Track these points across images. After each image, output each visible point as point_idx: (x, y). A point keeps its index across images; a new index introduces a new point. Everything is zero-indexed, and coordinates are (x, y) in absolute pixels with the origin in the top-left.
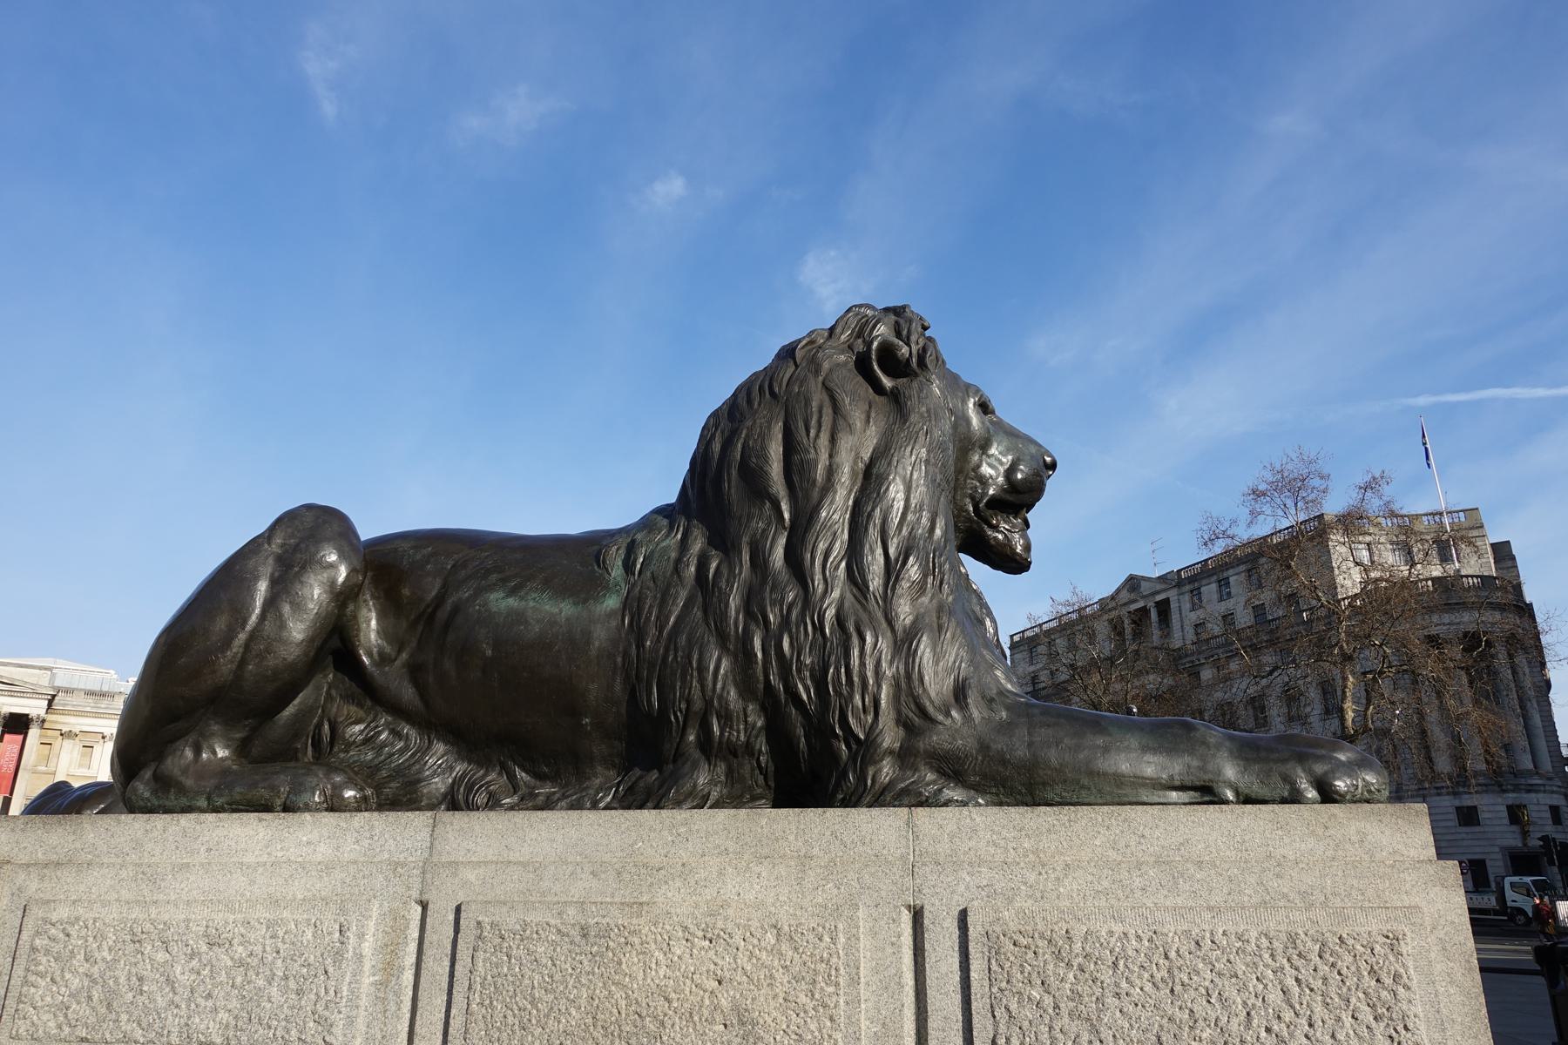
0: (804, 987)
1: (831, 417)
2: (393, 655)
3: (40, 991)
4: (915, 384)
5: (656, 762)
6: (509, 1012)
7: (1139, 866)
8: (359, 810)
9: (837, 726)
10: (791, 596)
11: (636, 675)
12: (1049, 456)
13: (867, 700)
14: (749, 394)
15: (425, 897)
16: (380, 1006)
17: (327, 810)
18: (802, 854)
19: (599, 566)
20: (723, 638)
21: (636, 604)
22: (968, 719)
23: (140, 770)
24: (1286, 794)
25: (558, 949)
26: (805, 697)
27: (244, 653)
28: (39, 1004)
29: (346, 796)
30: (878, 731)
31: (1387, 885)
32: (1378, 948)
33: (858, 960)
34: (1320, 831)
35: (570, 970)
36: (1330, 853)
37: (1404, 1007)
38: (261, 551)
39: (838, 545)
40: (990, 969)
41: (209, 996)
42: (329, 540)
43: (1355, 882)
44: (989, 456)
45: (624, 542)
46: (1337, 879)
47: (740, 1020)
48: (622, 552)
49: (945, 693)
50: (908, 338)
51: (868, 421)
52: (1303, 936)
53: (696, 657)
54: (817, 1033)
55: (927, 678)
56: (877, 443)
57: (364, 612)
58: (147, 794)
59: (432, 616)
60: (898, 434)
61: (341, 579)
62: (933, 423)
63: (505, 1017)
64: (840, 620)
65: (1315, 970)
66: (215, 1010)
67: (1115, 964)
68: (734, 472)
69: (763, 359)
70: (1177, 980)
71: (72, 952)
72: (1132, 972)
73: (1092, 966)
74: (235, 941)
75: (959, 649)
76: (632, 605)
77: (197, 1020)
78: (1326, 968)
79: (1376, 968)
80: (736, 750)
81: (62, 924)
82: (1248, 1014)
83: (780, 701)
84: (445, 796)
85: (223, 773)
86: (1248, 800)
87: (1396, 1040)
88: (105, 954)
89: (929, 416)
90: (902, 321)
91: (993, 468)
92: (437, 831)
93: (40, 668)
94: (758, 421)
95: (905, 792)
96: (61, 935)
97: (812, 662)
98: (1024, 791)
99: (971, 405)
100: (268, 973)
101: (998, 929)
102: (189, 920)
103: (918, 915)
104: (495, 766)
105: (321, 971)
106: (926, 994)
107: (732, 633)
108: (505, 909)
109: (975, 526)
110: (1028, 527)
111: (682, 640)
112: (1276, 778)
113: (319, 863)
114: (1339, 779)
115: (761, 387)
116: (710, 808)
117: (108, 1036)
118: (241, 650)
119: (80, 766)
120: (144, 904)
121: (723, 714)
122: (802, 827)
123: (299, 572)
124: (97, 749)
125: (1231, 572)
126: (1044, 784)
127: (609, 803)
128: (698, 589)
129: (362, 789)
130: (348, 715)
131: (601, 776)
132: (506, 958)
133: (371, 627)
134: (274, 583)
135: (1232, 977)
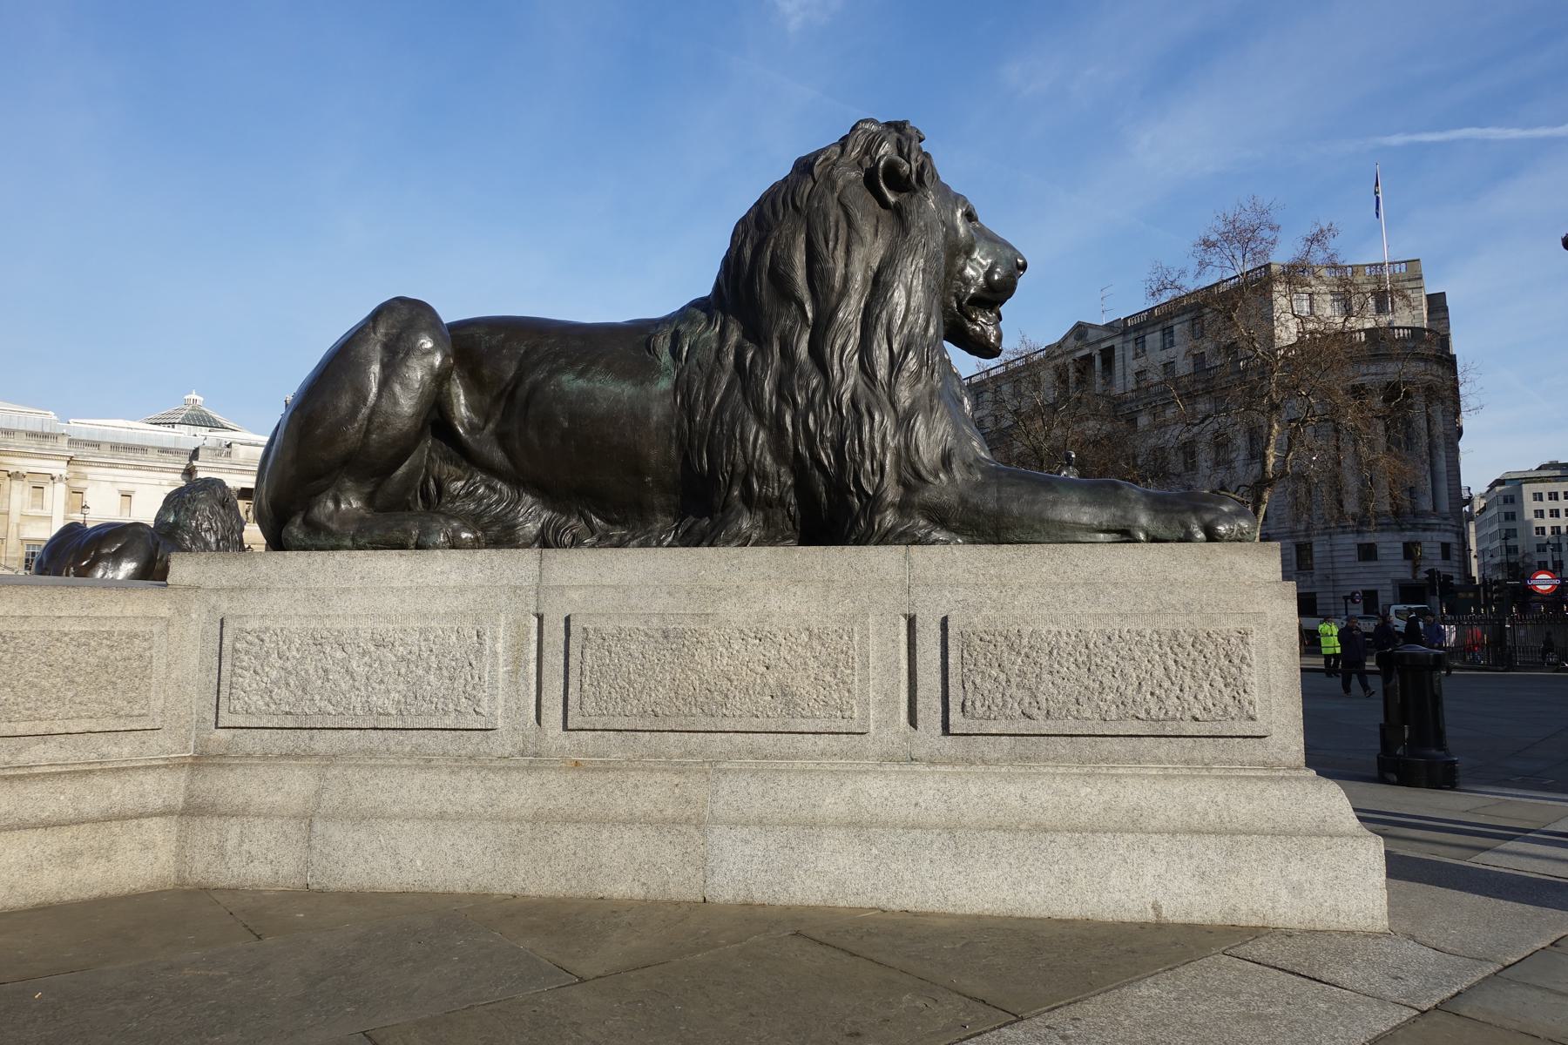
0: (829, 669)
1: (846, 231)
2: (481, 425)
3: (247, 679)
4: (915, 200)
5: (708, 511)
6: (613, 690)
7: (1072, 586)
8: (473, 548)
9: (852, 485)
10: (815, 382)
11: (689, 443)
12: (1021, 259)
14: (774, 205)
15: (540, 611)
17: (450, 548)
19: (650, 352)
20: (759, 416)
21: (685, 387)
22: (952, 480)
23: (291, 517)
24: (1182, 535)
25: (647, 646)
26: (826, 463)
27: (368, 425)
28: (248, 689)
30: (883, 489)
32: (1233, 640)
33: (868, 652)
34: (1203, 562)
36: (1208, 577)
37: (1245, 678)
38: (368, 340)
39: (852, 341)
40: (962, 657)
41: (382, 682)
42: (425, 330)
44: (972, 260)
46: (1211, 594)
47: (783, 693)
48: (668, 341)
49: (935, 459)
51: (876, 235)
52: (1182, 632)
53: (738, 430)
54: (838, 701)
55: (921, 448)
58: (301, 536)
59: (512, 395)
62: (930, 236)
63: (610, 693)
64: (854, 402)
65: (1188, 655)
67: (1051, 653)
68: (764, 277)
69: (784, 169)
71: (267, 652)
72: (1062, 657)
73: (1035, 653)
74: (397, 644)
75: (946, 425)
76: (682, 386)
80: (771, 503)
81: (255, 633)
82: (1140, 684)
83: (807, 465)
84: (537, 537)
86: (1154, 539)
88: (295, 653)
89: (926, 230)
90: (903, 139)
91: (975, 269)
92: (544, 563)
94: (784, 233)
95: (904, 534)
96: (256, 640)
98: (992, 533)
99: (959, 214)
100: (425, 665)
101: (969, 630)
102: (357, 629)
103: (911, 622)
104: (575, 513)
105: (466, 664)
106: (916, 674)
107: (767, 411)
108: (604, 619)
109: (957, 320)
110: (1001, 319)
111: (727, 416)
113: (454, 587)
114: (1221, 525)
116: (752, 545)
117: (307, 710)
118: (366, 423)
119: (33, 506)
121: (761, 475)
122: (827, 559)
123: (402, 358)
124: (48, 489)
125: (1176, 320)
126: (1007, 529)
128: (737, 374)
129: (474, 532)
130: (449, 474)
131: (661, 522)
132: (607, 653)
134: (384, 367)
135: (1131, 660)
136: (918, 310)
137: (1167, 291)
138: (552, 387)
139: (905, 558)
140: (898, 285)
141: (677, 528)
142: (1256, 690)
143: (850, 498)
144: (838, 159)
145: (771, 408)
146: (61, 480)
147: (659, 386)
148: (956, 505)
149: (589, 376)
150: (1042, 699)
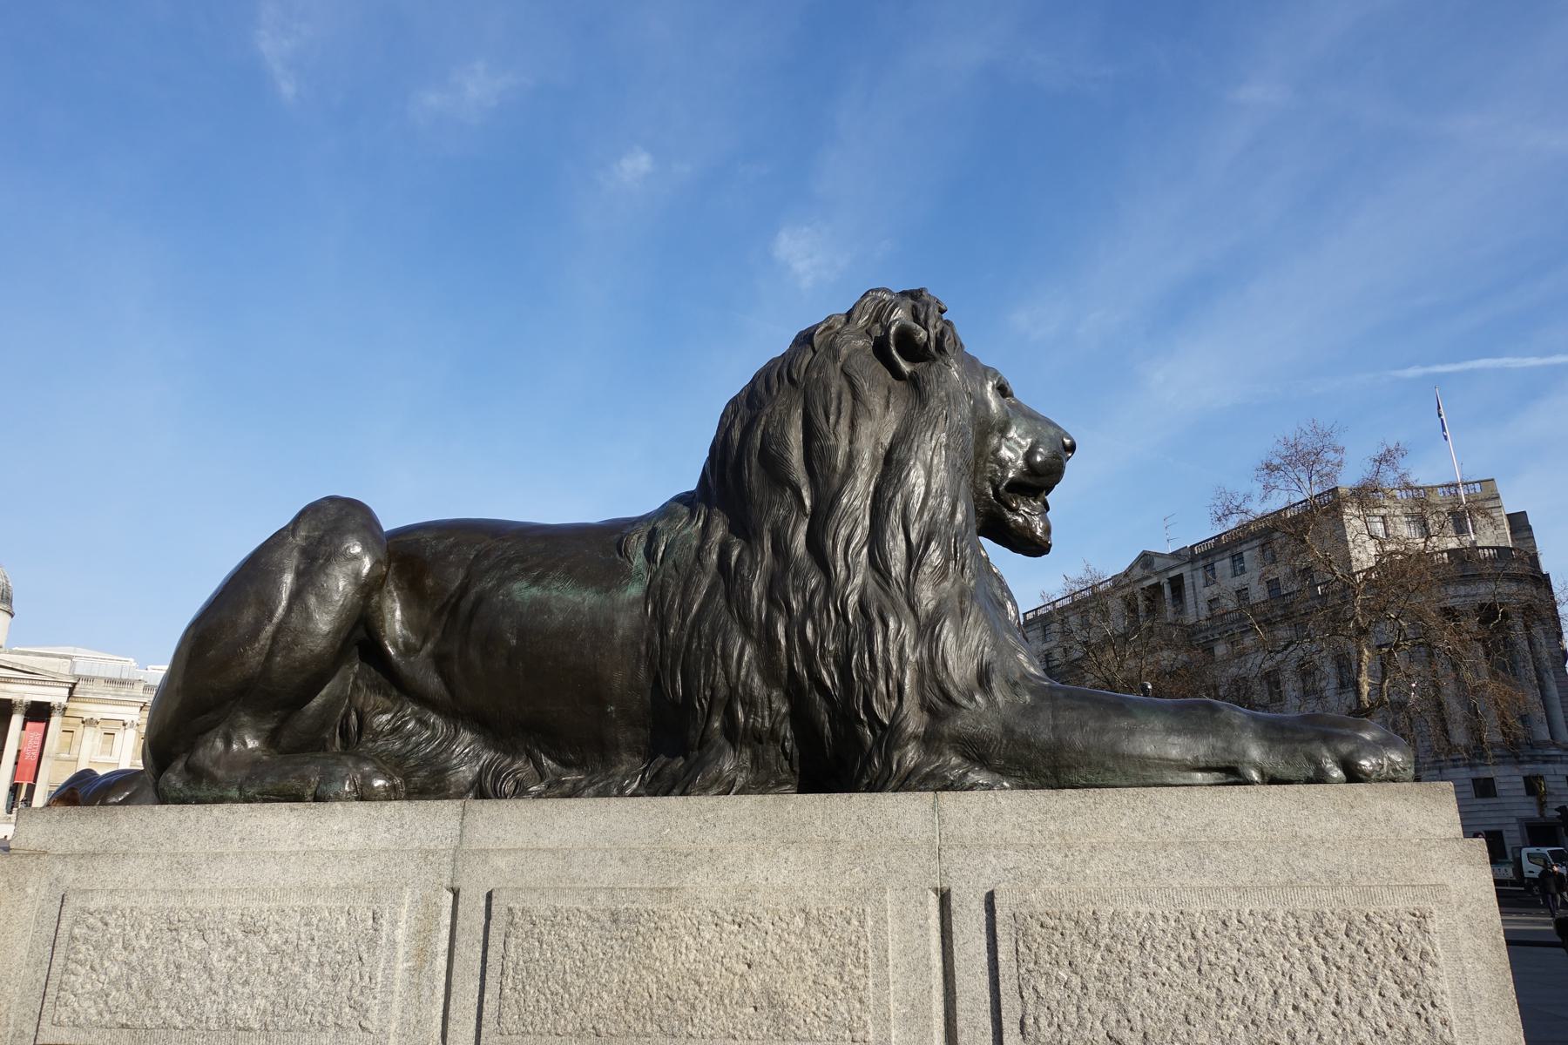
0: (833, 969)
1: (850, 403)
2: (418, 644)
3: (80, 979)
4: (934, 368)
5: (683, 749)
6: (542, 996)
7: (1165, 846)
8: (388, 799)
9: (861, 712)
10: (813, 583)
11: (661, 663)
12: (1068, 438)
13: (891, 685)
14: (767, 381)
15: (456, 885)
16: (414, 991)
17: (357, 799)
18: (829, 838)
19: (621, 554)
20: (746, 626)
22: (992, 703)
23: (172, 761)
24: (1311, 774)
25: (589, 935)
26: (829, 683)
27: (272, 645)
28: (80, 991)
29: (376, 785)
30: (902, 716)
31: (1414, 862)
32: (1404, 926)
33: (886, 943)
34: (1346, 811)
35: (601, 955)
36: (1356, 832)
37: (1432, 984)
38: (285, 544)
39: (859, 531)
40: (1017, 950)
41: (246, 983)
42: (353, 532)
43: (1381, 861)
44: (1008, 440)
45: (645, 530)
46: (1363, 858)
47: (770, 1002)
48: (644, 540)
49: (968, 677)
50: (926, 322)
51: (887, 407)
52: (1330, 915)
54: (846, 1015)
55: (950, 663)
56: (897, 429)
57: (388, 602)
58: (179, 785)
59: (456, 607)
60: (918, 419)
61: (365, 571)
62: (953, 407)
63: (538, 1001)
64: (863, 606)
65: (1342, 948)
66: (253, 996)
67: (1142, 945)
68: (754, 460)
69: (780, 345)
70: (1204, 960)
71: (110, 940)
72: (1159, 952)
73: (1119, 946)
74: (270, 930)
75: (982, 633)
76: (655, 593)
77: (235, 1006)
78: (1353, 946)
79: (1402, 945)
81: (99, 913)
82: (1275, 992)
83: (804, 687)
84: (472, 784)
85: (254, 765)
86: (1273, 780)
87: (1424, 1016)
88: (143, 942)
90: (919, 305)
91: (1013, 451)
92: (467, 819)
93: (61, 657)
94: (777, 408)
95: (931, 776)
96: (100, 924)
97: (836, 648)
98: (1049, 774)
99: (989, 387)
100: (303, 960)
101: (1025, 911)
103: (944, 898)
105: (355, 958)
106: (954, 976)
107: (755, 620)
108: (535, 896)
109: (994, 509)
110: (1048, 509)
111: (706, 628)
112: (1300, 758)
113: (351, 852)
114: (1365, 758)
115: (779, 374)
116: (736, 794)
117: (148, 1022)
118: (269, 642)
119: (102, 753)
120: (180, 893)
122: (829, 812)
123: (322, 565)
124: (119, 736)
125: (1245, 547)
126: (1069, 767)
127: (635, 790)
128: (720, 576)
129: (391, 779)
130: (375, 705)
131: (627, 763)
132: (537, 944)
133: (395, 618)
134: (299, 575)
135: (1259, 956)
136: (941, 492)
137: (1234, 516)
138: (501, 597)
139: (934, 809)
140: (915, 464)
141: (644, 771)
142: (1450, 1004)
143: (860, 728)
144: (842, 328)
146: (132, 726)
147: (627, 594)
148: (999, 736)
150: (1134, 1014)
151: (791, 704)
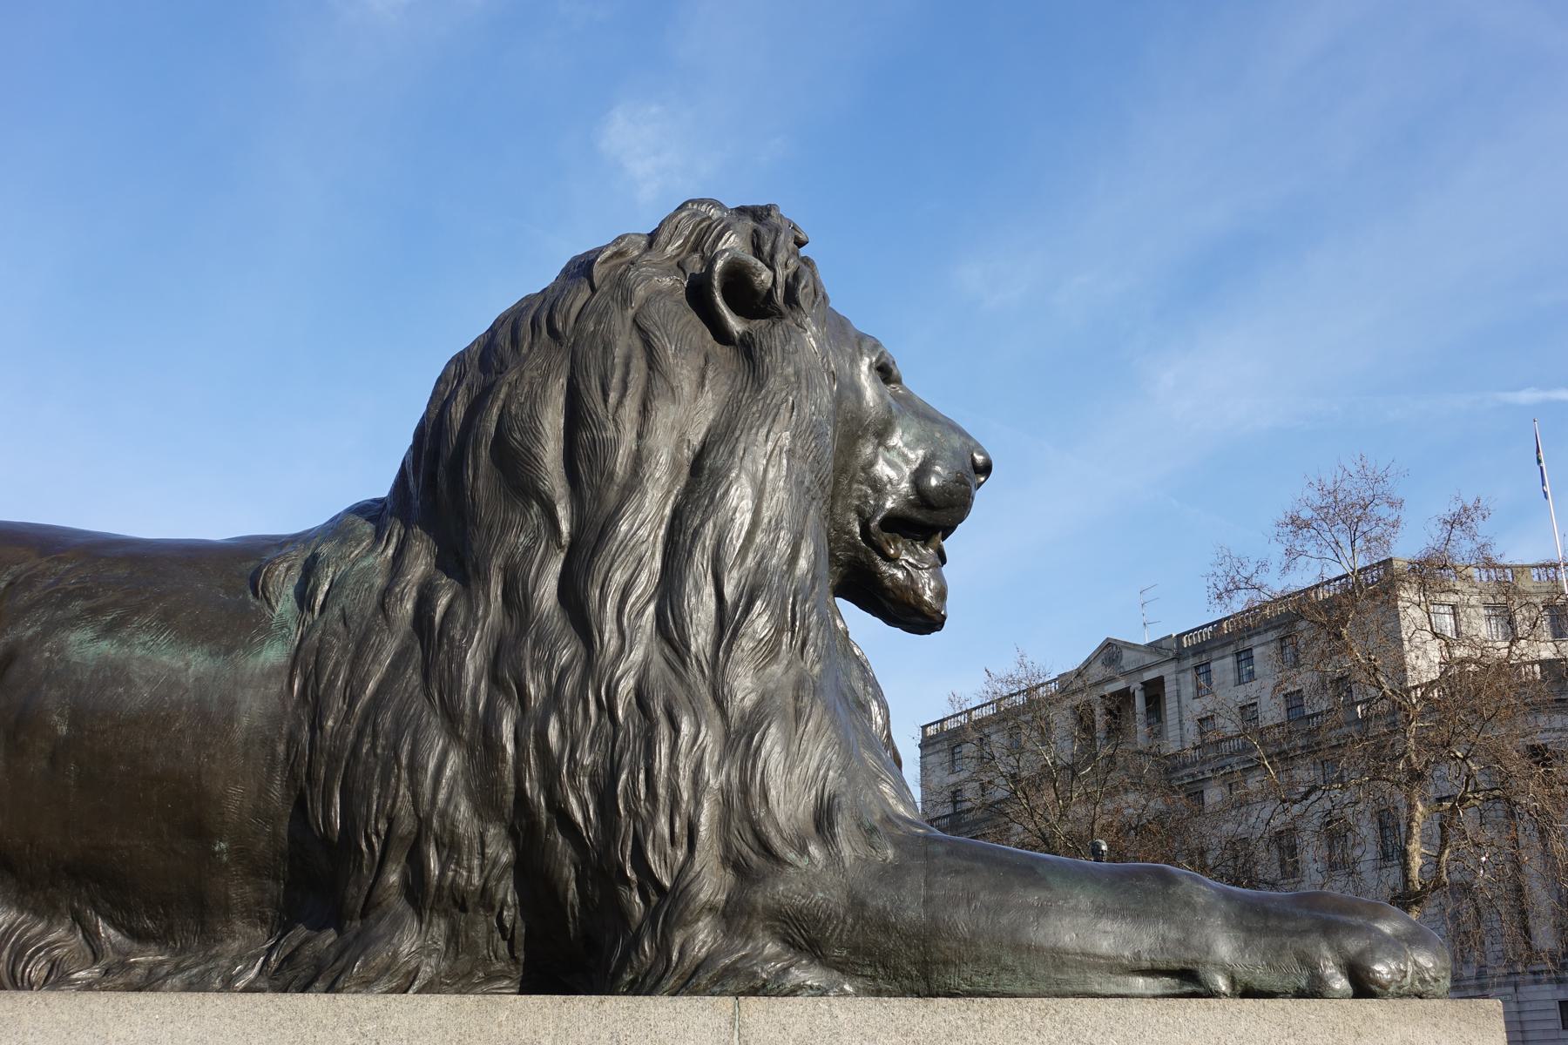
1: (643, 373)
4: (778, 331)
10: (565, 656)
11: (308, 774)
12: (980, 453)
13: (677, 825)
19: (256, 594)
20: (451, 718)
21: (313, 659)
22: (834, 859)
26: (579, 817)
30: (692, 874)
39: (644, 577)
44: (888, 449)
45: (299, 557)
48: (296, 574)
49: (800, 816)
50: (772, 257)
51: (702, 384)
55: (773, 792)
56: (713, 420)
60: (748, 407)
62: (804, 392)
64: (641, 697)
68: (484, 453)
69: (541, 276)
75: (826, 748)
80: (464, 900)
83: (540, 823)
86: (1249, 992)
89: (798, 381)
90: (763, 230)
94: (527, 374)
95: (731, 971)
97: (594, 762)
99: (865, 365)
104: (63, 916)
107: (467, 711)
109: (862, 557)
110: (944, 561)
111: (386, 720)
112: (1290, 959)
114: (1380, 961)
115: (535, 323)
116: (419, 992)
121: (446, 840)
122: (565, 1025)
125: (1255, 640)
126: (946, 963)
127: (253, 982)
136: (777, 524)
138: (47, 654)
139: (732, 1024)
140: (738, 476)
141: (270, 951)
143: (622, 889)
144: (640, 256)
145: (475, 704)
147: (261, 658)
148: (841, 911)
149: (124, 634)
151: (516, 847)
